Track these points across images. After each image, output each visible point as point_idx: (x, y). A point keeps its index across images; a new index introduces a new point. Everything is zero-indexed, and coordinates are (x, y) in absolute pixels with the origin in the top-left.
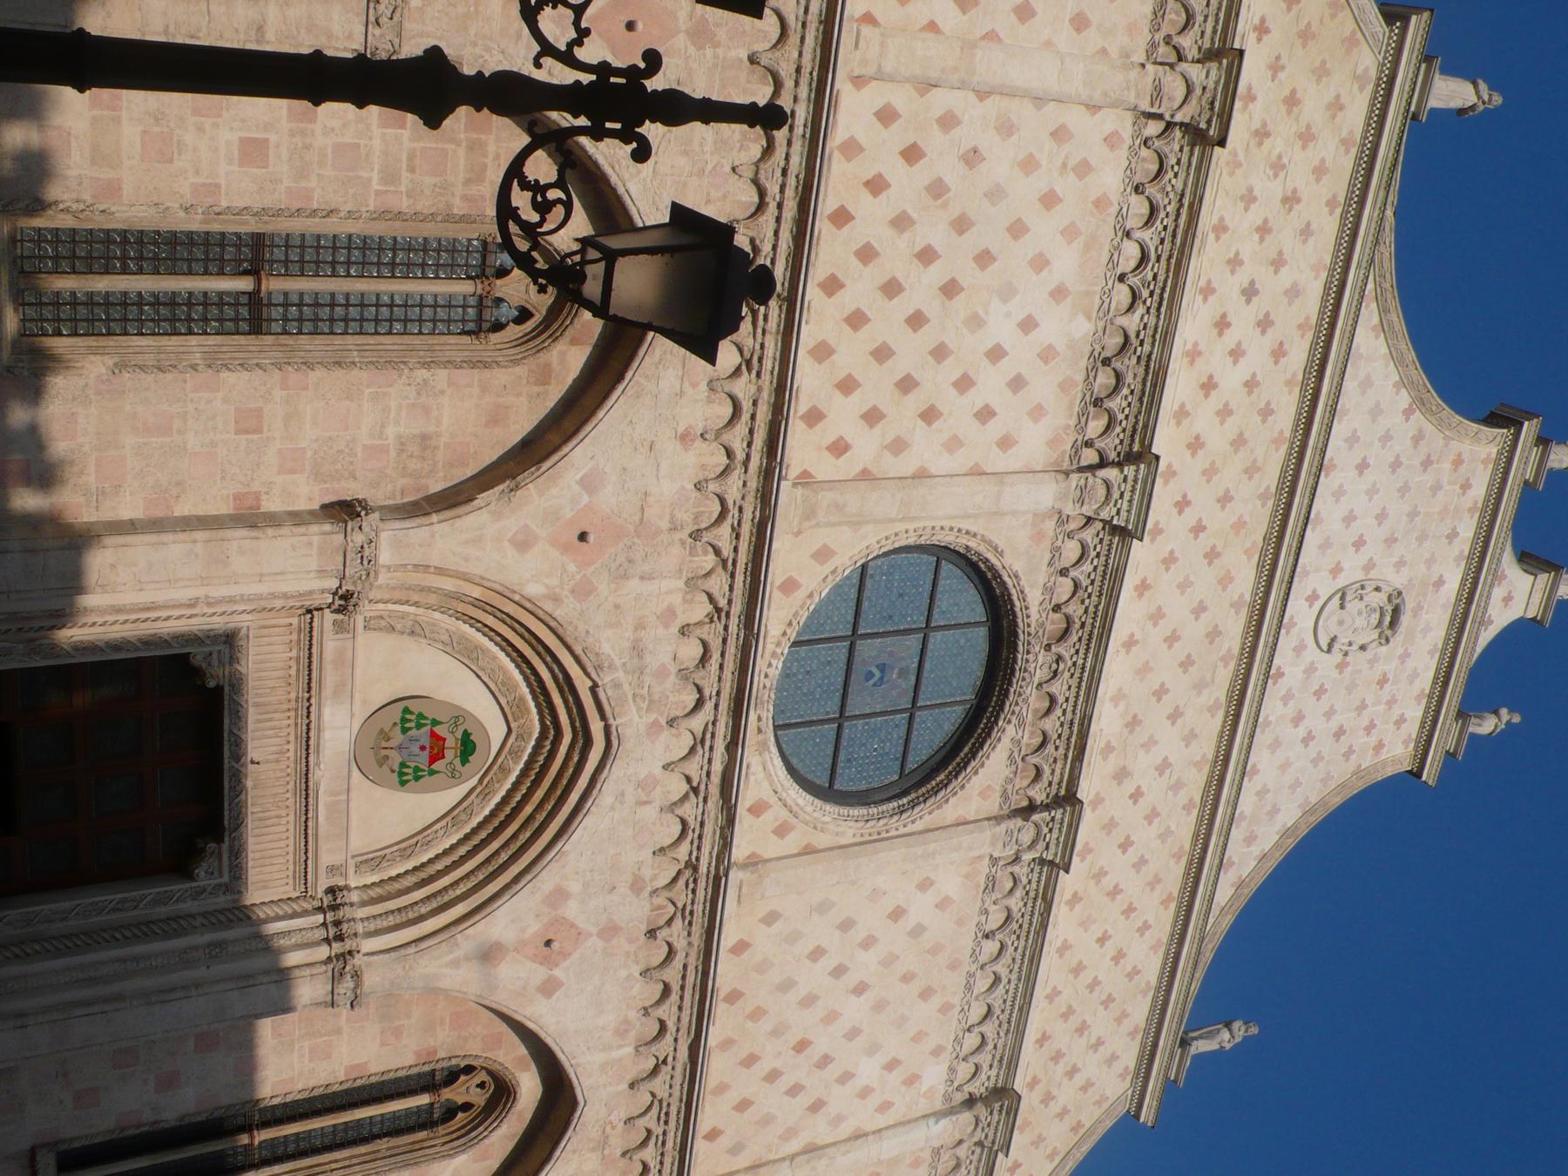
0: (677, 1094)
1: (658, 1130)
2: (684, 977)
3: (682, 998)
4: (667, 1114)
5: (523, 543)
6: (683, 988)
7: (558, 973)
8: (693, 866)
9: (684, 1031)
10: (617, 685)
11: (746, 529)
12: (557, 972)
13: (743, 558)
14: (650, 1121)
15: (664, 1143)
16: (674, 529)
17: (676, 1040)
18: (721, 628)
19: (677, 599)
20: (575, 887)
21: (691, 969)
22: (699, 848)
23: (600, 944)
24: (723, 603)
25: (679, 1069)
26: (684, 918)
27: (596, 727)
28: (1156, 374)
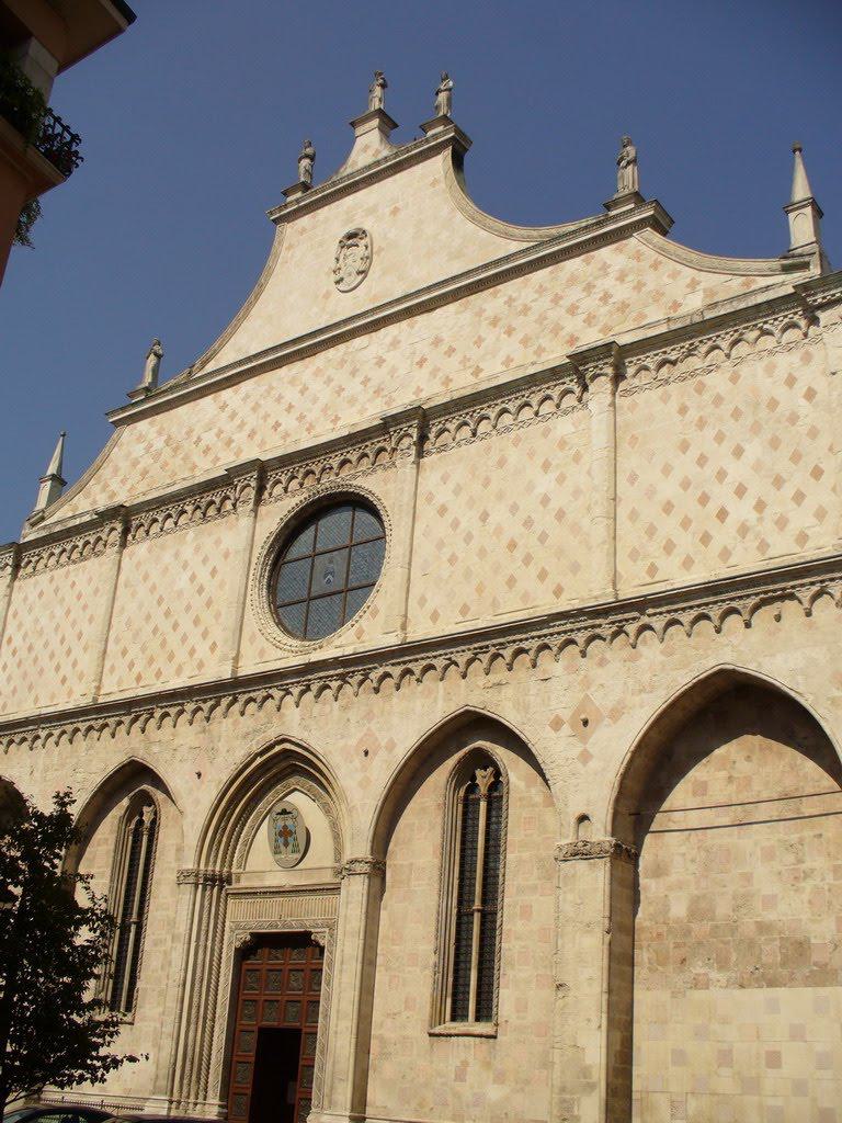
1: (493, 650)
3: (410, 661)
4: (481, 648)
5: (197, 802)
7: (383, 744)
10: (258, 743)
12: (383, 744)
14: (486, 658)
16: (204, 731)
19: (229, 721)
20: (341, 743)
22: (332, 676)
27: (277, 748)
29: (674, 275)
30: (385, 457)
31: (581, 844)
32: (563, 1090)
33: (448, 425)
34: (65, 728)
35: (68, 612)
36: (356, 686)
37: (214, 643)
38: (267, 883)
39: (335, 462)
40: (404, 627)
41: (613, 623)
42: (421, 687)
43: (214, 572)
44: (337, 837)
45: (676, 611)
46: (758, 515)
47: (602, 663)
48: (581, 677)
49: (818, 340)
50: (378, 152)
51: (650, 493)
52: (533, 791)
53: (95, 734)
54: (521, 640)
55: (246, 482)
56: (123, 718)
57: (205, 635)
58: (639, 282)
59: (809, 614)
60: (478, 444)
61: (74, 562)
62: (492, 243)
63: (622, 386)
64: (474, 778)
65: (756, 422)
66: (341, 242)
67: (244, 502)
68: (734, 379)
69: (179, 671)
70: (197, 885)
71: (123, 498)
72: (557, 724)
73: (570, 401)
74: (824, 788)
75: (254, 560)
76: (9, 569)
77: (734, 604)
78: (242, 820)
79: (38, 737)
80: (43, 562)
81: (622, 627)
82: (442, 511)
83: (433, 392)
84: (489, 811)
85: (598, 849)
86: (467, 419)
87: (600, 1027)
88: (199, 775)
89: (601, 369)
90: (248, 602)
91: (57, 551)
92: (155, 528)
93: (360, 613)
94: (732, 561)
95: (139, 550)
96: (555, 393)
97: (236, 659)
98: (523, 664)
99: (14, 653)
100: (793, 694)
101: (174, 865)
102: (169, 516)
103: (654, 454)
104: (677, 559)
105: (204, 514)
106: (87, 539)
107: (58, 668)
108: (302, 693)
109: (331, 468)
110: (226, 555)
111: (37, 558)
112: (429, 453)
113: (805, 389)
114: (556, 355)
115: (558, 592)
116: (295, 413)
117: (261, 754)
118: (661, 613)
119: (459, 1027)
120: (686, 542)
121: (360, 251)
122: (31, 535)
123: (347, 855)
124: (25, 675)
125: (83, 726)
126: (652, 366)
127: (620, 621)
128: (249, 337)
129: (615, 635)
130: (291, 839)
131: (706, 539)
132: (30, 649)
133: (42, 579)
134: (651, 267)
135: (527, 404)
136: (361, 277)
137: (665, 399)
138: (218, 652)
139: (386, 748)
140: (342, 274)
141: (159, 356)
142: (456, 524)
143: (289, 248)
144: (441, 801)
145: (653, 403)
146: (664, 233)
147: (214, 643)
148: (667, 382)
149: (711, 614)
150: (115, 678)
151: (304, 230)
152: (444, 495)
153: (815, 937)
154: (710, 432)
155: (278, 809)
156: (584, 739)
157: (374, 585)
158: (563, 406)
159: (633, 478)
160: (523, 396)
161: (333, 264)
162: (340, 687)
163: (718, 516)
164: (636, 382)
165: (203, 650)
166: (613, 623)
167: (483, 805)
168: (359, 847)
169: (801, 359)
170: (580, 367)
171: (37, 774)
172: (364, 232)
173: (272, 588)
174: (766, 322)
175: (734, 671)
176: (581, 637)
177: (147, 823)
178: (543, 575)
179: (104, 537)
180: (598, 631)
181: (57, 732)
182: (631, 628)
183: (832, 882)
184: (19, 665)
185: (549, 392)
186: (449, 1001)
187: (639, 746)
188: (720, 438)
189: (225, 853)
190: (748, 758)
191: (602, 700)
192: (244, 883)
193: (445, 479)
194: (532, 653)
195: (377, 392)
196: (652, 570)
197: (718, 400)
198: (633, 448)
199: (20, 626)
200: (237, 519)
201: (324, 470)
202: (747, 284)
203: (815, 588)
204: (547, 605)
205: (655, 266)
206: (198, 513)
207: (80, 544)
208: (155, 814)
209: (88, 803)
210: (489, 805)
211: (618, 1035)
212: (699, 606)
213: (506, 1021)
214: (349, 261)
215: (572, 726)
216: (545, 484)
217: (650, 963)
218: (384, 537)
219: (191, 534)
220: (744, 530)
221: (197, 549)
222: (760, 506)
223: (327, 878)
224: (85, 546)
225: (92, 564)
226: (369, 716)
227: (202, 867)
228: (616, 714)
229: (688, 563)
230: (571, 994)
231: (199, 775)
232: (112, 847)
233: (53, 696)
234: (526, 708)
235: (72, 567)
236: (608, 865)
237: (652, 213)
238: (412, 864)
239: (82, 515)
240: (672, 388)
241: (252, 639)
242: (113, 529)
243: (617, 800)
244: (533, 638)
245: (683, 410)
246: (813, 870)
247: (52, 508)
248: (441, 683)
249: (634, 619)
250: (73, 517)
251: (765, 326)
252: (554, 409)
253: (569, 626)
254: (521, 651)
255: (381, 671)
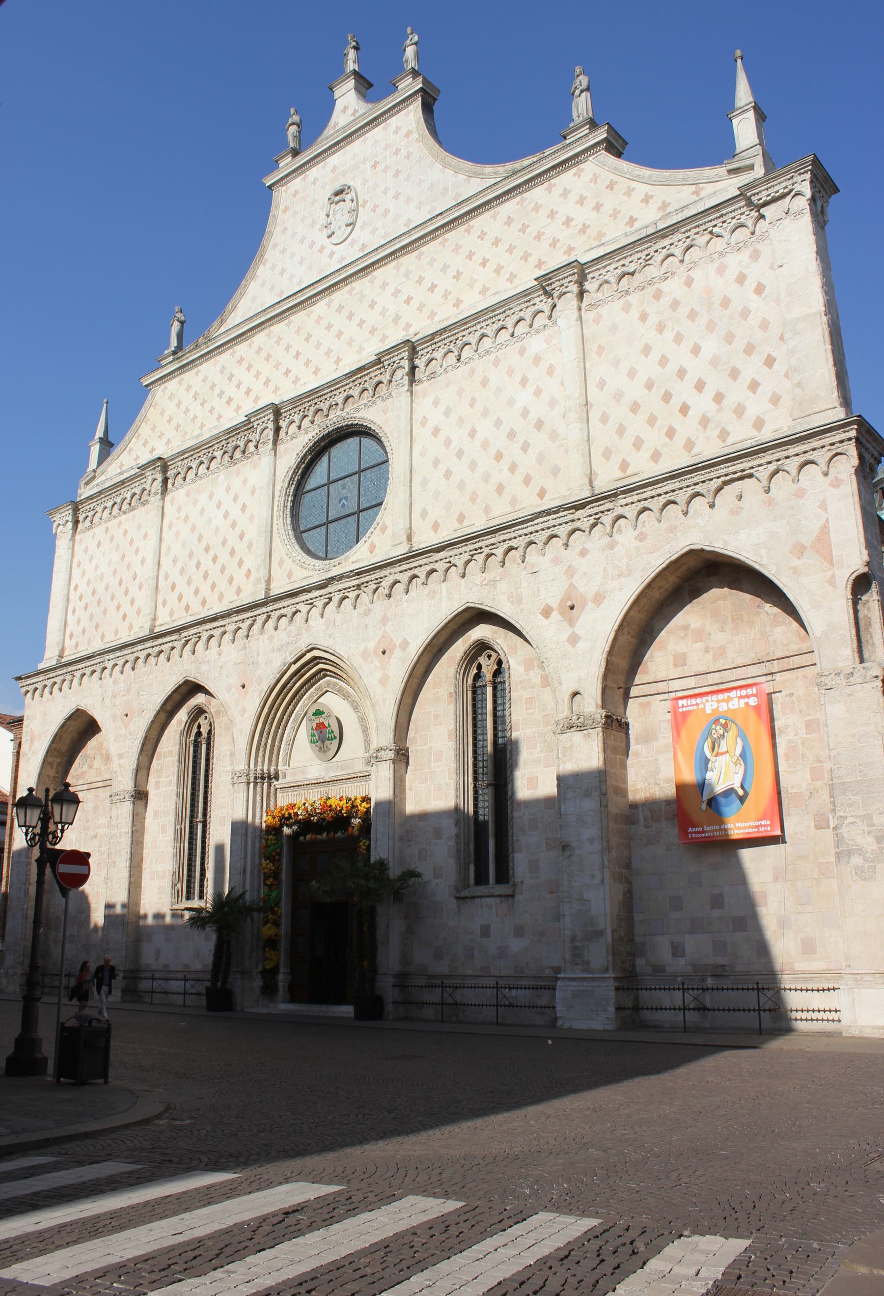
0: (464, 549)
1: (486, 551)
2: (406, 570)
3: (416, 567)
4: (476, 550)
6: (410, 569)
8: (358, 587)
9: (430, 560)
10: (291, 654)
11: (240, 617)
13: (249, 614)
14: (480, 558)
15: (493, 544)
17: (436, 561)
18: (272, 614)
19: (266, 636)
21: (401, 569)
23: (390, 623)
24: (265, 616)
25: (452, 553)
26: (380, 582)
28: (228, 433)
29: (629, 192)
30: (383, 389)
31: (575, 718)
32: (573, 939)
33: (435, 355)
34: (127, 657)
35: (123, 557)
36: (371, 594)
37: (249, 571)
38: (309, 777)
39: (340, 399)
40: (409, 539)
41: (590, 516)
42: (427, 589)
43: (244, 508)
44: (365, 730)
45: (646, 499)
46: (718, 407)
47: (583, 553)
48: (565, 568)
49: (765, 236)
50: (355, 111)
51: (618, 396)
52: (531, 673)
53: (152, 660)
54: (510, 540)
55: (264, 425)
56: (176, 644)
57: (240, 563)
58: (597, 203)
59: (768, 491)
60: (464, 369)
61: (125, 513)
62: (462, 181)
63: (586, 301)
64: (479, 667)
65: (711, 321)
66: (329, 199)
67: (264, 443)
68: (689, 282)
69: (221, 597)
70: (248, 783)
71: (163, 451)
72: (547, 612)
73: (541, 320)
74: (793, 651)
75: (277, 493)
76: (70, 525)
77: (698, 488)
78: (282, 724)
79: (105, 668)
80: (98, 515)
81: (599, 519)
82: (436, 432)
83: (421, 326)
84: (495, 695)
85: (590, 722)
86: (452, 347)
87: (603, 880)
88: (243, 687)
89: (566, 287)
90: (275, 530)
91: (109, 504)
92: (191, 475)
93: (371, 530)
94: (695, 451)
95: (178, 495)
96: (528, 314)
97: (268, 582)
98: (515, 560)
99: (81, 598)
100: (757, 567)
101: (229, 768)
102: (202, 463)
103: (619, 361)
104: (646, 453)
105: (232, 457)
106: (133, 491)
107: (118, 607)
108: (327, 604)
109: (337, 405)
110: (253, 492)
111: (93, 512)
112: (420, 381)
113: (754, 285)
114: (527, 281)
115: (542, 494)
116: (302, 360)
117: (295, 662)
118: (632, 503)
119: (481, 890)
120: (654, 438)
121: (348, 205)
122: (85, 492)
123: (374, 746)
124: (91, 617)
125: (142, 655)
126: (613, 280)
127: (597, 514)
128: (257, 293)
129: (594, 525)
130: (327, 736)
131: (671, 433)
132: (94, 593)
133: (98, 530)
134: (607, 187)
135: (503, 328)
136: (350, 228)
137: (627, 308)
138: (253, 577)
139: (400, 646)
140: (333, 228)
141: (182, 323)
142: (448, 442)
143: (285, 211)
144: (452, 690)
145: (615, 314)
146: (619, 155)
147: (249, 571)
148: (627, 293)
149: (678, 500)
150: (167, 610)
151: (296, 193)
152: (436, 417)
153: (792, 787)
154: (669, 335)
155: (313, 710)
156: (571, 622)
157: (381, 504)
158: (535, 325)
159: (602, 384)
160: (499, 320)
161: (323, 220)
162: (358, 596)
163: (680, 411)
164: (600, 295)
165: (239, 576)
166: (590, 516)
167: (489, 690)
168: (384, 737)
169: (750, 257)
170: (545, 285)
171: (107, 701)
172: (349, 187)
173: (295, 515)
174: (716, 226)
175: (702, 550)
176: (563, 531)
177: (205, 734)
178: (527, 480)
179: (148, 488)
180: (577, 524)
181: (121, 662)
182: (607, 519)
183: (805, 736)
184: (86, 608)
185: (522, 314)
186: (472, 867)
187: (621, 626)
188: (678, 339)
189: (271, 753)
190: (722, 630)
191: (586, 588)
192: (289, 778)
193: (436, 403)
194: (521, 550)
195: (372, 332)
196: (624, 465)
197: (675, 305)
198: (600, 356)
199: (83, 573)
200: (260, 459)
201: (331, 406)
202: (696, 193)
203: (772, 467)
204: (531, 504)
205: (611, 186)
206: (226, 457)
207: (128, 496)
208: (210, 725)
209: (153, 722)
210: (495, 689)
211: (620, 888)
212: (666, 493)
213: (522, 882)
214: (338, 216)
215: (562, 613)
216: (524, 398)
217: (645, 821)
218: (387, 461)
219: (222, 476)
220: (705, 422)
221: (228, 489)
222: (719, 398)
223: (360, 767)
224: (132, 498)
225: (140, 513)
226: (384, 620)
227: (252, 766)
228: (598, 599)
229: (656, 456)
230: (577, 852)
231: (243, 687)
232: (177, 758)
233: (116, 633)
234: (520, 601)
235: (123, 517)
236: (601, 734)
237: (605, 135)
238: (430, 749)
239: (127, 471)
240: (633, 298)
241: (281, 563)
242: (155, 480)
243: (605, 676)
244: (520, 536)
245: (644, 317)
246: (787, 727)
247: (102, 468)
248: (444, 585)
249: (609, 510)
250: (121, 473)
251: (715, 230)
252: (527, 329)
253: (551, 523)
254: (511, 549)
255: (391, 579)
